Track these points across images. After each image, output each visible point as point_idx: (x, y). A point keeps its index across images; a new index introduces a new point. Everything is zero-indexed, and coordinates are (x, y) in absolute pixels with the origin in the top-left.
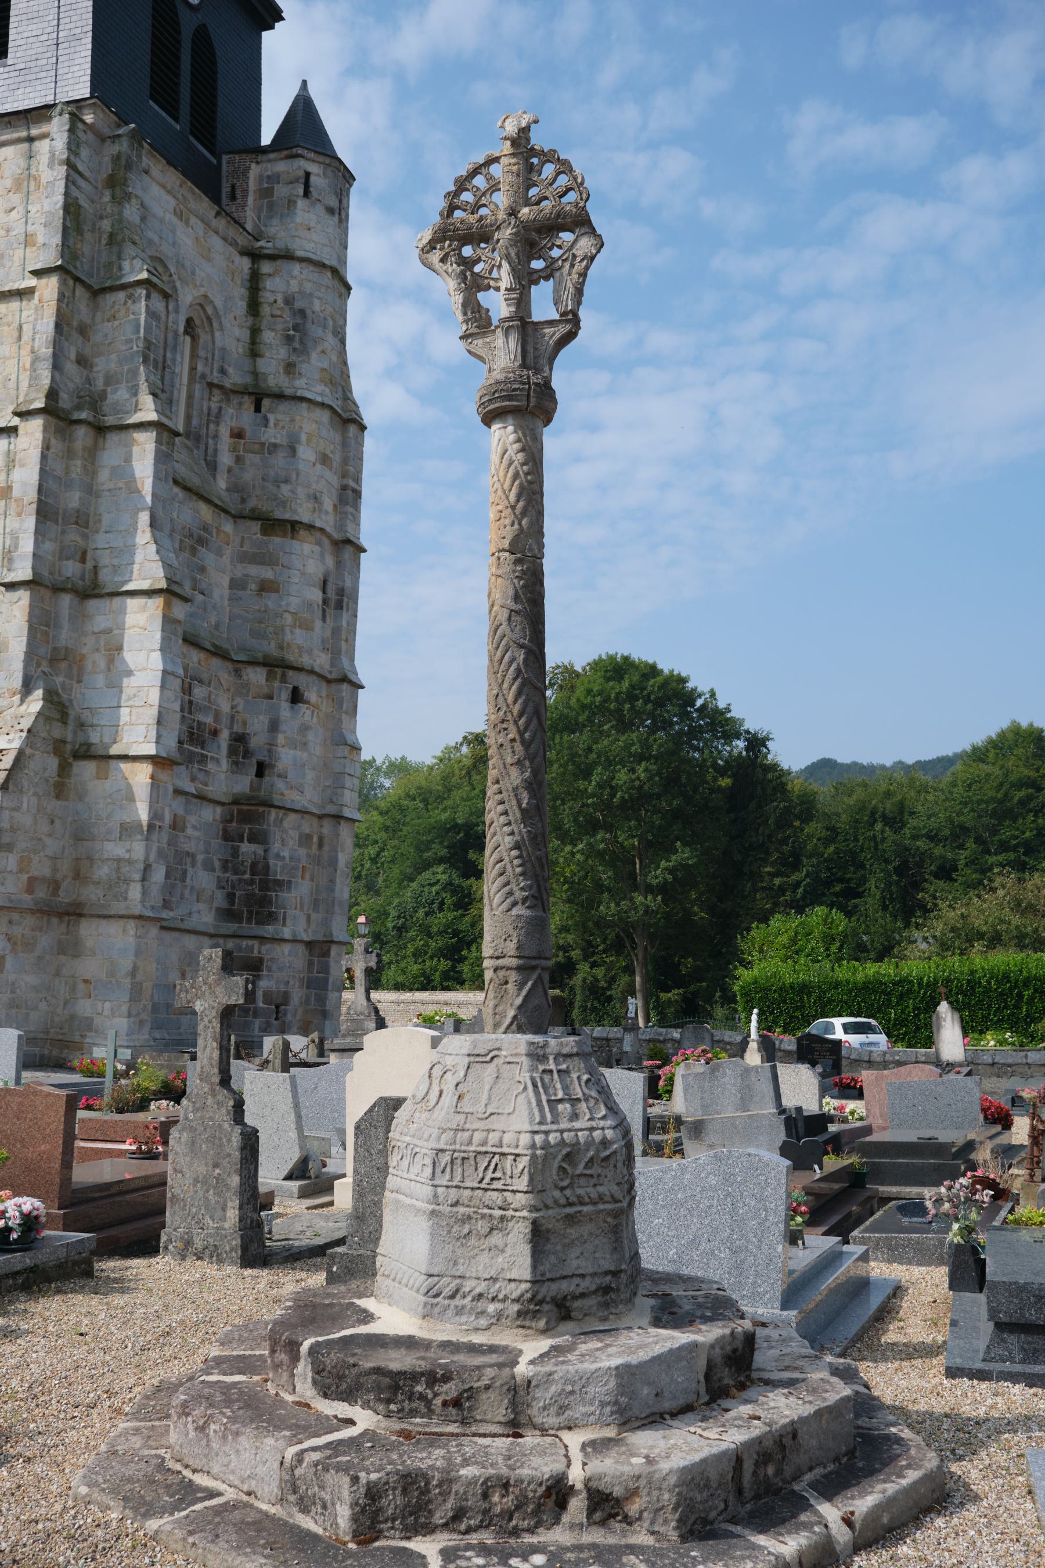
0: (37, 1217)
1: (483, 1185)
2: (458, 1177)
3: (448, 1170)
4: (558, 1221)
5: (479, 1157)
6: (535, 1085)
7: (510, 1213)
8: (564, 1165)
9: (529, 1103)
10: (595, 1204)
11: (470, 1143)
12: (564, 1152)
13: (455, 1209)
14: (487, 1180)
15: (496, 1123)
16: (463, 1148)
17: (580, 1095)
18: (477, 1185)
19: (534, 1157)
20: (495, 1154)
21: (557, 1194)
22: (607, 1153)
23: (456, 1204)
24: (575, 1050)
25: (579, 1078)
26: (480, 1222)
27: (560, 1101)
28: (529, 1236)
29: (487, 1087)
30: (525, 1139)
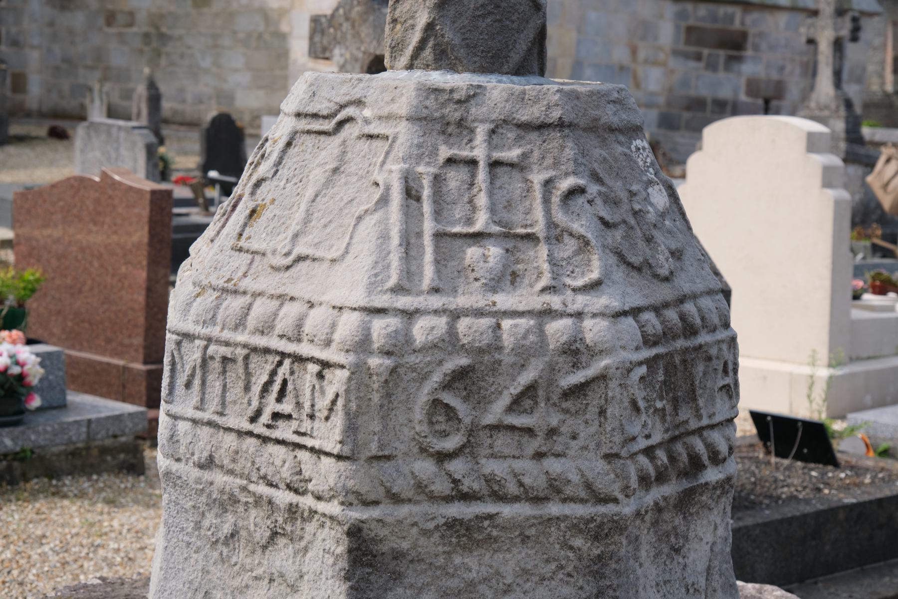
0: (21, 377)
1: (259, 429)
2: (213, 404)
3: (197, 382)
4: (426, 533)
5: (255, 359)
6: (411, 194)
7: (307, 502)
8: (448, 398)
9: (385, 237)
10: (538, 500)
11: (240, 324)
12: (450, 365)
13: (207, 475)
14: (265, 418)
15: (301, 283)
16: (227, 335)
17: (539, 229)
18: (246, 426)
19: (359, 372)
20: (283, 355)
21: (425, 468)
22: (578, 377)
23: (209, 464)
24: (556, 114)
25: (548, 184)
26: (253, 513)
27: (477, 237)
28: (343, 564)
29: (310, 193)
30: (348, 325)
